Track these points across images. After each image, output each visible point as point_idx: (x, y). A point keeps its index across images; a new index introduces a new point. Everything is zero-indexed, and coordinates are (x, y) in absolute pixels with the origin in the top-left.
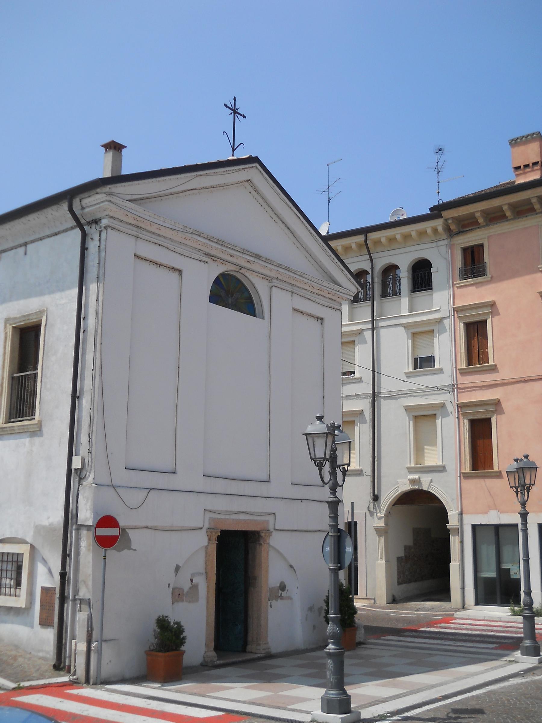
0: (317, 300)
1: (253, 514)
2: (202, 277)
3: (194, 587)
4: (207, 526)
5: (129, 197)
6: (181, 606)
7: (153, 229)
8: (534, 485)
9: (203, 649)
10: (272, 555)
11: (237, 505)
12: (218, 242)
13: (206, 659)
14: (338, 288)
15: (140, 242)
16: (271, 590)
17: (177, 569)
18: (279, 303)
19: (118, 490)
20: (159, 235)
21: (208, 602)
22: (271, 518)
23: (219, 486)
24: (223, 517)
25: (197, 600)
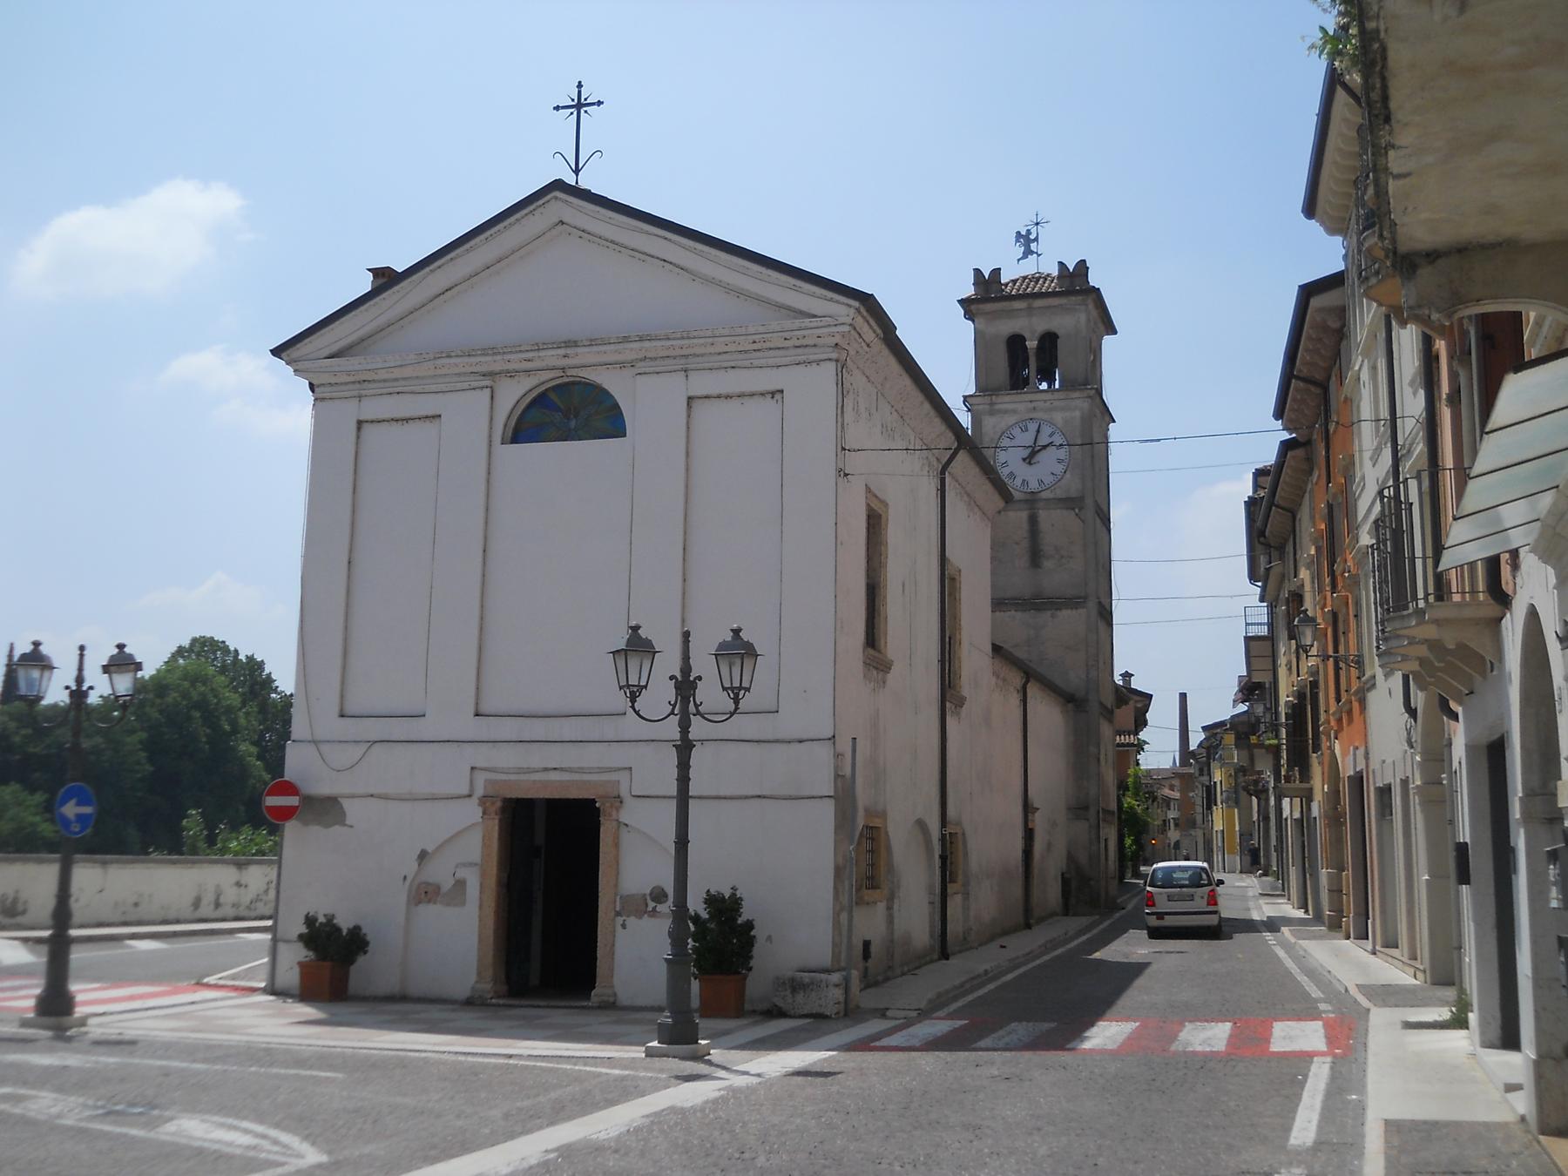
0: (756, 362)
1: (581, 770)
2: (472, 418)
3: (460, 884)
4: (479, 792)
5: (327, 352)
6: (430, 913)
7: (383, 375)
8: (748, 690)
9: (473, 978)
10: (626, 838)
11: (538, 758)
12: (485, 352)
13: (290, 975)
14: (815, 322)
15: (365, 401)
16: (626, 900)
17: (423, 855)
18: (648, 401)
19: (325, 748)
20: (396, 380)
21: (481, 907)
22: (623, 777)
23: (508, 729)
24: (513, 777)
25: (463, 903)
